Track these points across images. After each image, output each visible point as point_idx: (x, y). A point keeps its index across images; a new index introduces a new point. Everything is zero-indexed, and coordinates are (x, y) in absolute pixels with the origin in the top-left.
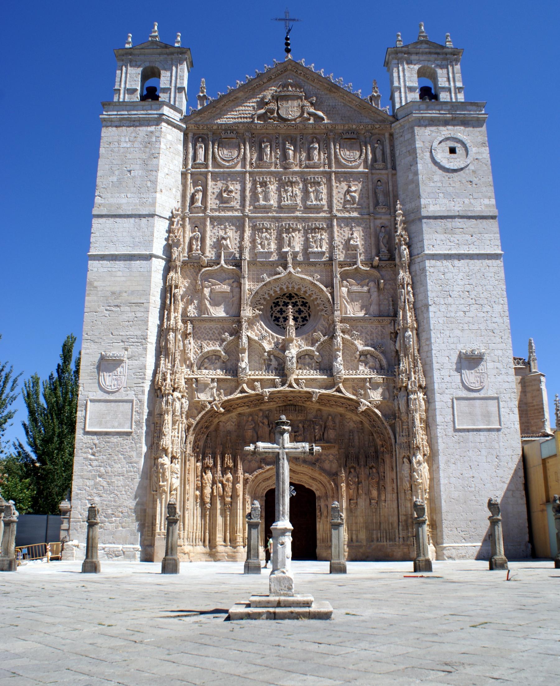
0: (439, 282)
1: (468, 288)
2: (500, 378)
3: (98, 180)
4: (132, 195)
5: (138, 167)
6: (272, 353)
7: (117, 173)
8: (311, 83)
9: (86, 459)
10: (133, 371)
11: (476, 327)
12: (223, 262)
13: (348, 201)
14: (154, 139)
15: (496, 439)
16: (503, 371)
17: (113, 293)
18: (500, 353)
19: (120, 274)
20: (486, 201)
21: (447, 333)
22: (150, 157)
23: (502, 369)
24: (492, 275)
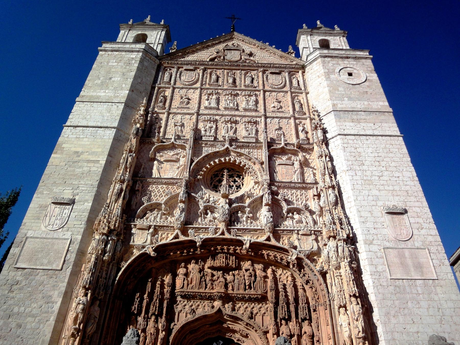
0: (353, 154)
1: (378, 159)
2: (423, 232)
3: (87, 82)
4: (110, 91)
5: (118, 76)
6: (208, 208)
8: (248, 45)
10: (76, 214)
11: (391, 188)
12: (173, 140)
13: (274, 107)
14: (133, 62)
15: (434, 290)
16: (425, 225)
17: (77, 152)
18: (418, 210)
19: (85, 139)
20: (381, 103)
21: (367, 193)
22: (128, 71)
23: (423, 224)
24: (397, 150)
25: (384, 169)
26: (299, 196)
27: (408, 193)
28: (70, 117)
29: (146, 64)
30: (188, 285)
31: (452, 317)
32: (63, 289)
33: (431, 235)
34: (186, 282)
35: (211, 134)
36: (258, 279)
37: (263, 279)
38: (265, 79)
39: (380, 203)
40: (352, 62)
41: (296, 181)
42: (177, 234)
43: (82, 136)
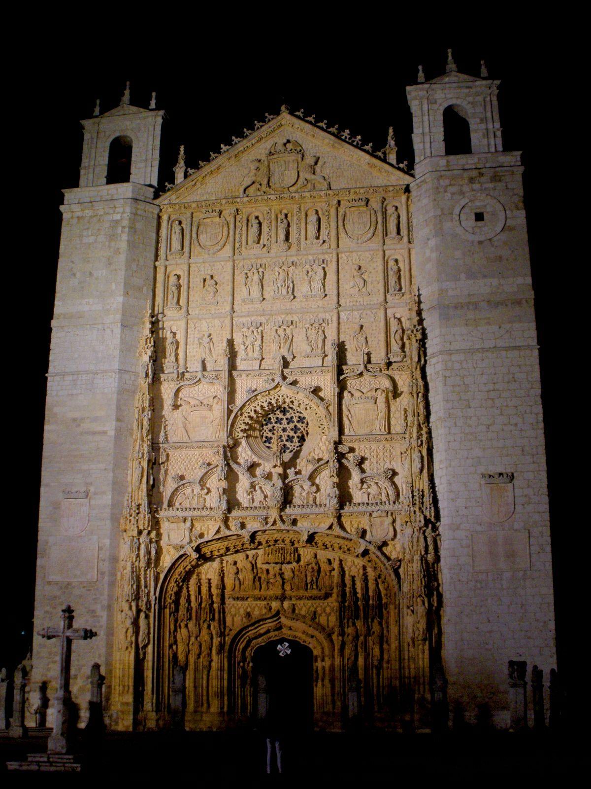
0: (457, 389)
7: (78, 275)
9: (46, 612)
14: (119, 230)
17: (74, 420)
20: (520, 280)
25: (499, 412)
26: (381, 454)
27: (523, 451)
28: (51, 358)
29: (139, 226)
30: (240, 584)
31: (535, 613)
32: (105, 603)
33: (539, 512)
34: (237, 583)
35: (255, 356)
36: (322, 574)
37: (328, 574)
38: (340, 223)
39: (482, 469)
40: (487, 185)
41: (379, 432)
42: (220, 528)
43: (75, 392)
